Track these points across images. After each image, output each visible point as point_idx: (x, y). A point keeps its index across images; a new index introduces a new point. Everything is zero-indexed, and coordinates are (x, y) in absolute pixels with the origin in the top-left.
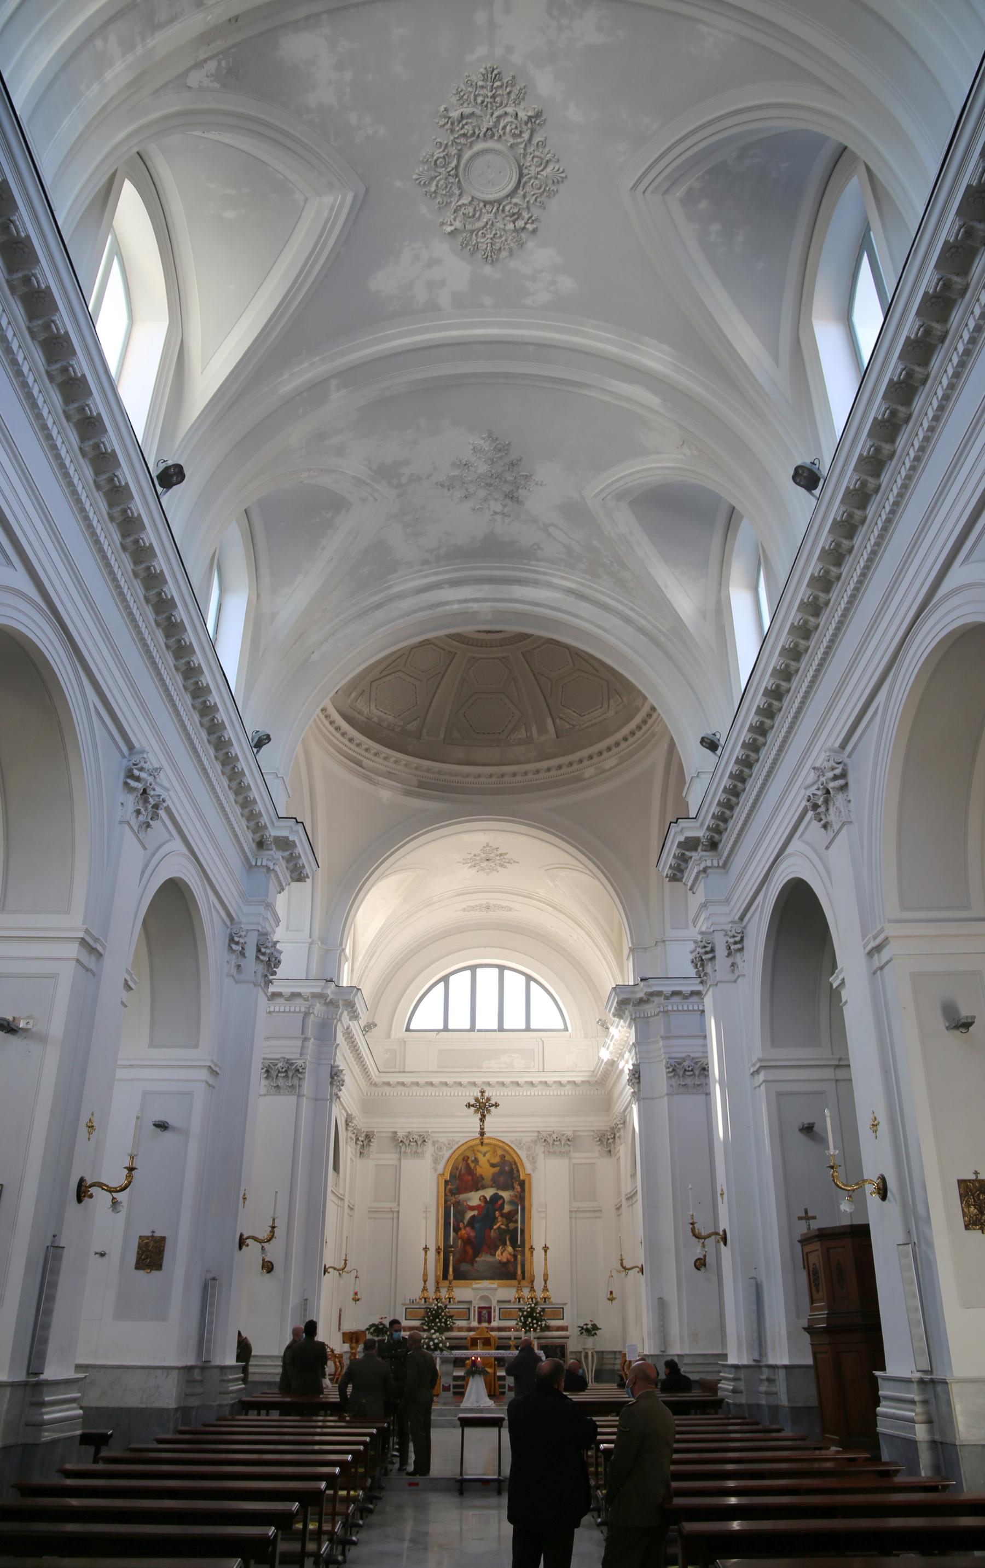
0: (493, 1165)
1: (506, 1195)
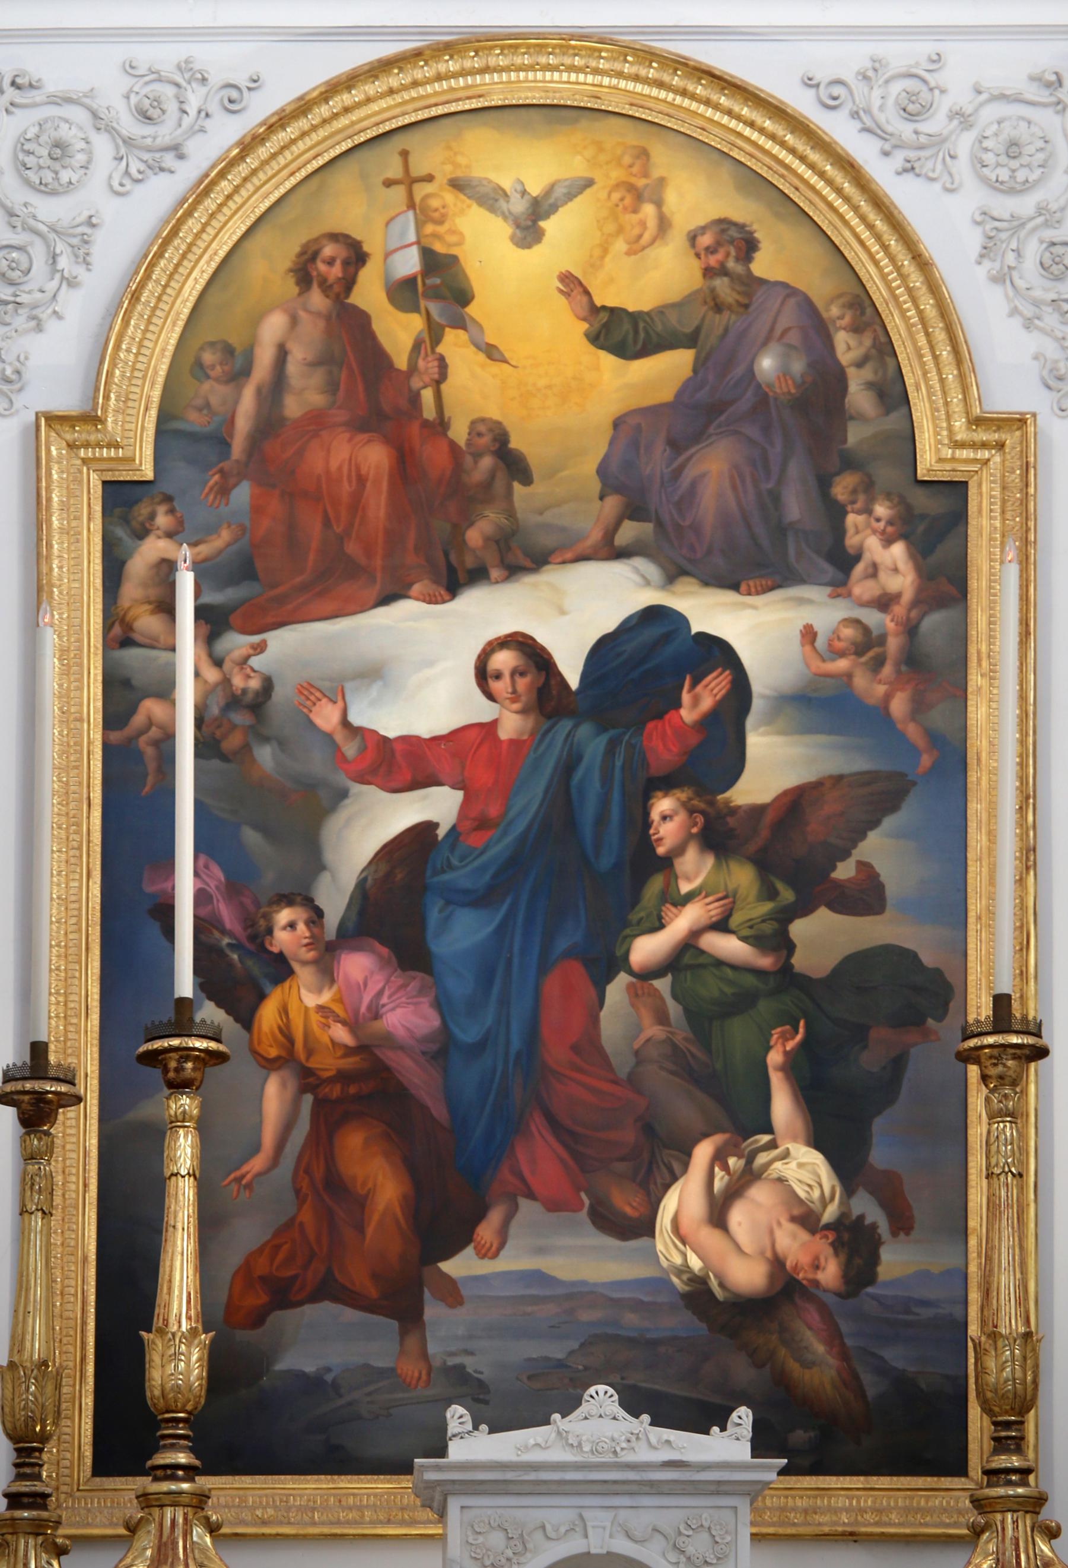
0: (620, 333)
1: (760, 630)
